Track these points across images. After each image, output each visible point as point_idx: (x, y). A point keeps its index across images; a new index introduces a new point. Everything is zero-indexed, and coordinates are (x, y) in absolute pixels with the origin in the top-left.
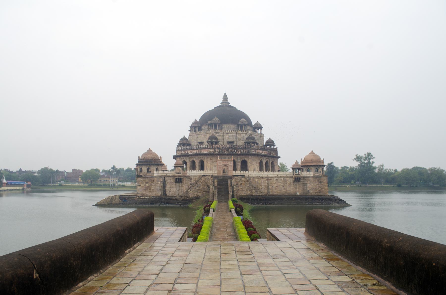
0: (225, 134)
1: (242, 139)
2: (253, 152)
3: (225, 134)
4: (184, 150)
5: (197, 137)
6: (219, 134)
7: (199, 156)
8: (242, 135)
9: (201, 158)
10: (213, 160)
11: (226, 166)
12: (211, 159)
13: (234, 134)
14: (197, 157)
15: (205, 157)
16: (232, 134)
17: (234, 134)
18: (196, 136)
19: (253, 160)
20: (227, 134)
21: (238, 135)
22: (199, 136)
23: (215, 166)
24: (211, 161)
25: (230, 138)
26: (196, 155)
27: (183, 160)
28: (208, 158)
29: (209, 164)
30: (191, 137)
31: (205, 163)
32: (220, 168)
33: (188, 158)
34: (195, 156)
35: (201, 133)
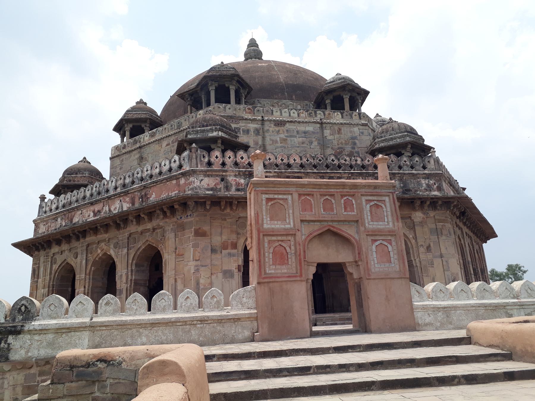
0: (270, 127)
1: (348, 148)
2: (429, 188)
3: (270, 127)
4: (68, 210)
5: (141, 159)
6: (242, 125)
7: (133, 228)
8: (347, 133)
9: (142, 235)
10: (217, 240)
11: (331, 234)
12: (199, 233)
13: (310, 128)
14: (123, 235)
15: (168, 224)
16: (302, 128)
17: (310, 128)
18: (135, 156)
19: (438, 232)
20: (280, 123)
21: (327, 132)
22: (147, 151)
23: (228, 274)
24: (203, 242)
25: (297, 140)
26: (121, 221)
27: (60, 259)
28: (182, 227)
29: (191, 265)
30: (117, 161)
31: (169, 260)
32: (281, 258)
33: (79, 245)
34: (113, 232)
35: (158, 137)
